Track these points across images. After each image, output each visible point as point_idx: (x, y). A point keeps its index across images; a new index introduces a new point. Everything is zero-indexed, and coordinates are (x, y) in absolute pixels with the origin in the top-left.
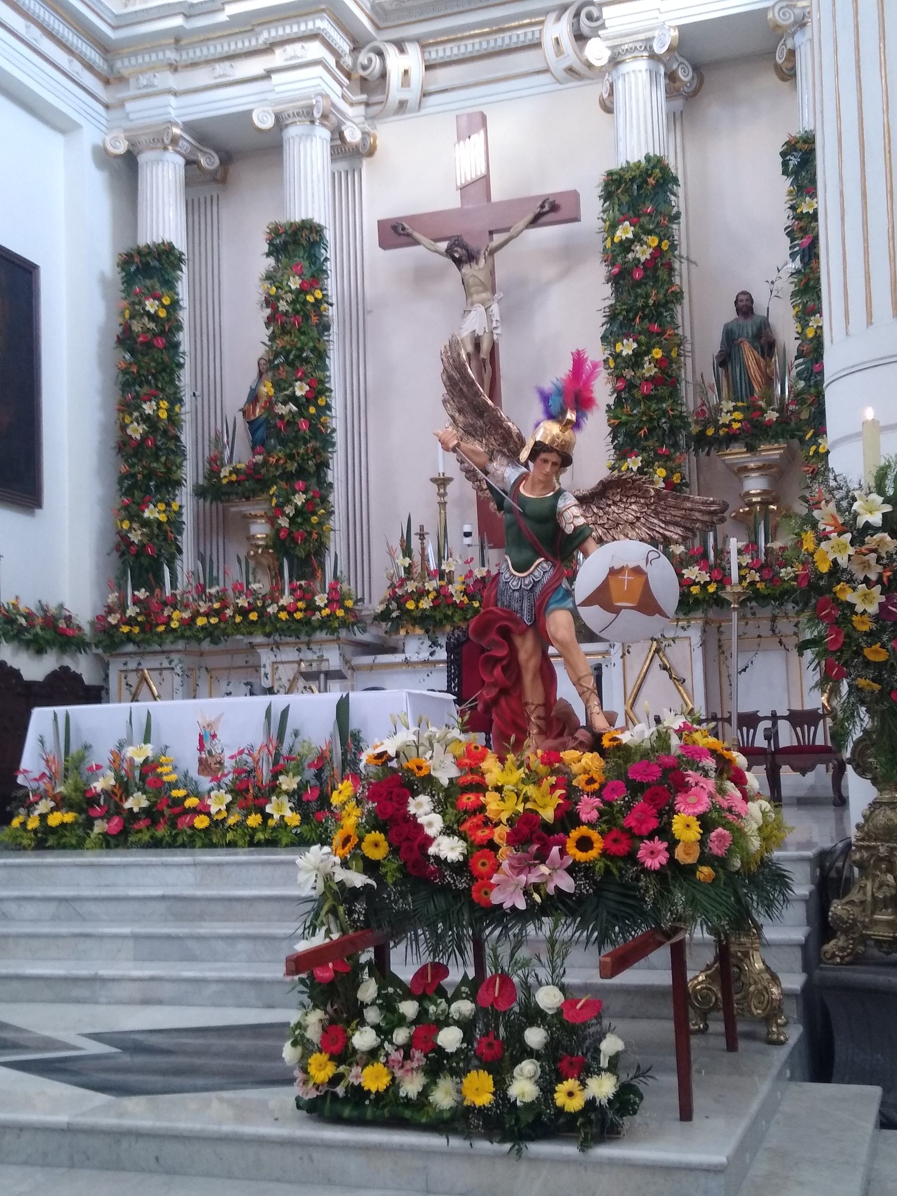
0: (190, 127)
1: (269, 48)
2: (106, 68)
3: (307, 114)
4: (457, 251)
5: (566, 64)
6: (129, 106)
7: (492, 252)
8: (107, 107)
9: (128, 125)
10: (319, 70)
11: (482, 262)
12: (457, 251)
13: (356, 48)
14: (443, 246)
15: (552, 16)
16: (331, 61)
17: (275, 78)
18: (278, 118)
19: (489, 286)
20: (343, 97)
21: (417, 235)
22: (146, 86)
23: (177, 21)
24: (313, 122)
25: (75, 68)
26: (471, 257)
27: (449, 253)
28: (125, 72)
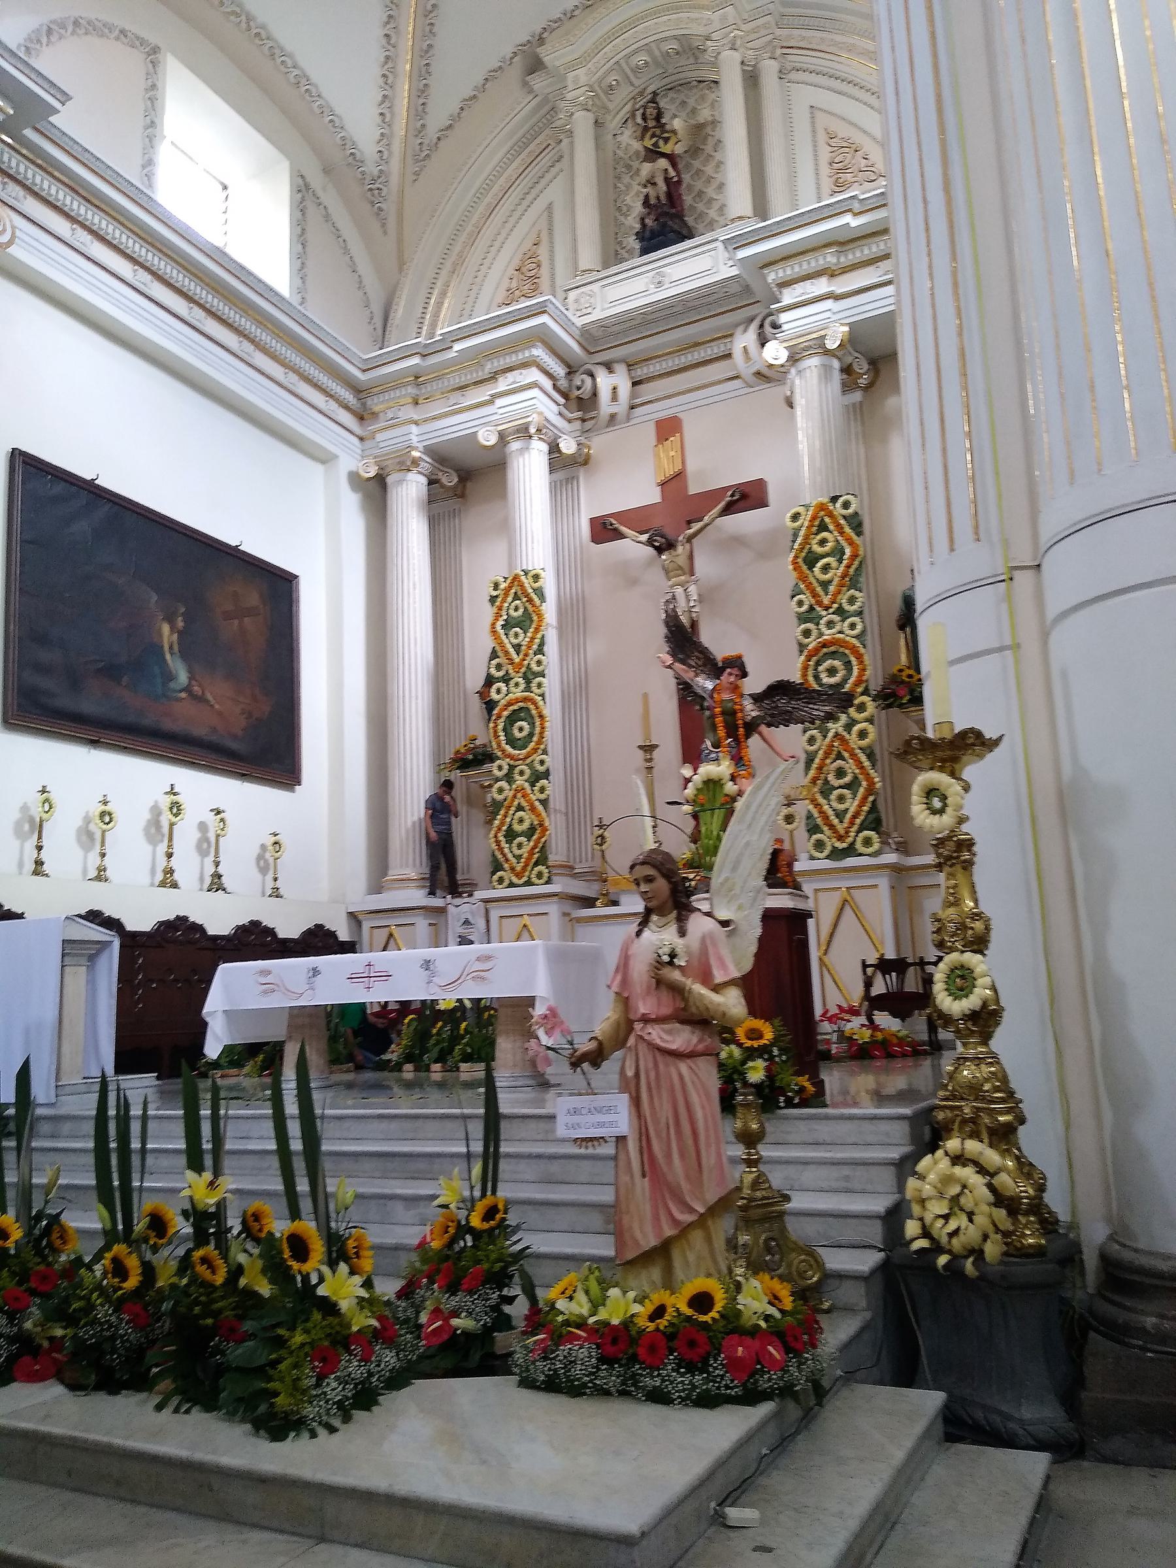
0: (428, 450)
1: (493, 377)
2: (359, 405)
3: (523, 432)
4: (655, 541)
5: (754, 369)
6: (380, 437)
7: (689, 539)
8: (361, 439)
9: (376, 451)
10: (535, 392)
11: (680, 549)
12: (655, 541)
13: (571, 372)
14: (644, 537)
15: (741, 328)
16: (547, 384)
17: (500, 402)
18: (502, 436)
19: (687, 569)
20: (560, 414)
21: (624, 529)
22: (392, 419)
23: (416, 360)
24: (530, 437)
25: (332, 407)
26: (670, 546)
27: (650, 542)
28: (376, 409)
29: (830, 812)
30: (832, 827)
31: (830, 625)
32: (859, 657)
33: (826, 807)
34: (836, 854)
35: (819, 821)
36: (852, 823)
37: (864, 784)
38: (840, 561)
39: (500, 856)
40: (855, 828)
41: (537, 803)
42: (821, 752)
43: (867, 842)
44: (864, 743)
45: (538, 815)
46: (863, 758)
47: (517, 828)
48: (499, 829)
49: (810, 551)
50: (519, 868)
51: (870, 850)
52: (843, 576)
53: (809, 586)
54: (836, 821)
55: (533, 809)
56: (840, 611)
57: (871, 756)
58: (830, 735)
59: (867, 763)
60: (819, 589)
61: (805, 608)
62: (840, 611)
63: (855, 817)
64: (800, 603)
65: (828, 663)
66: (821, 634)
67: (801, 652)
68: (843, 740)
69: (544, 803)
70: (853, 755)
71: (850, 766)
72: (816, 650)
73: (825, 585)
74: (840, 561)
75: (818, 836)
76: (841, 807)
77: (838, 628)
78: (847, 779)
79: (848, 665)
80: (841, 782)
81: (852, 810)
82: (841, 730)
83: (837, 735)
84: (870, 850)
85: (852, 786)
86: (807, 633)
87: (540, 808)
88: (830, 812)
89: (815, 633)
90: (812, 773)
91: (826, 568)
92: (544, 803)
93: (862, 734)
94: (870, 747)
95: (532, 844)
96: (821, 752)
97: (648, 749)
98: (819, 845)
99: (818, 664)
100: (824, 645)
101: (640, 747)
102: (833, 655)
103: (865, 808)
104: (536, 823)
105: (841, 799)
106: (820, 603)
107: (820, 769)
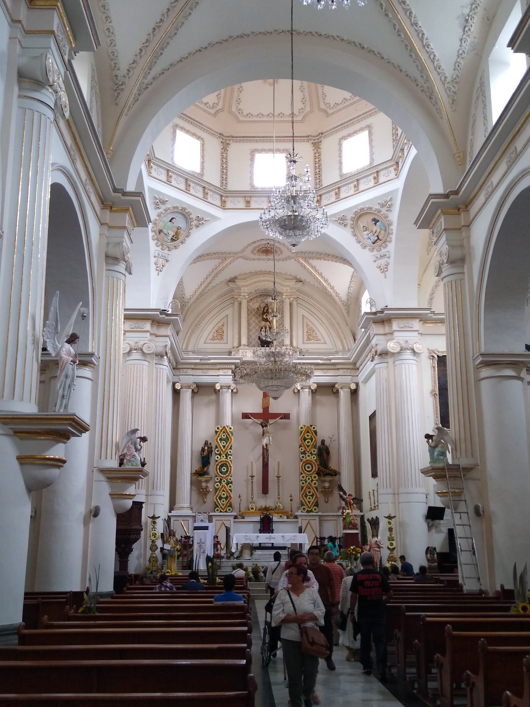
29: (307, 502)
30: (307, 505)
31: (309, 456)
32: (315, 465)
33: (306, 500)
34: (308, 512)
35: (304, 503)
36: (312, 504)
37: (315, 495)
38: (312, 441)
39: (217, 504)
40: (312, 506)
41: (228, 490)
42: (305, 487)
43: (315, 509)
44: (315, 486)
45: (229, 494)
46: (315, 489)
47: (223, 496)
48: (217, 496)
49: (305, 437)
50: (223, 507)
51: (316, 511)
52: (312, 445)
53: (304, 446)
54: (308, 504)
55: (227, 492)
56: (311, 453)
57: (317, 489)
58: (308, 483)
59: (316, 491)
60: (306, 447)
61: (303, 451)
62: (311, 453)
63: (313, 503)
64: (302, 449)
65: (308, 465)
66: (306, 458)
67: (301, 461)
68: (311, 485)
69: (231, 491)
70: (313, 488)
71: (312, 491)
72: (306, 461)
73: (308, 446)
74: (312, 441)
75: (304, 507)
76: (309, 500)
77: (310, 457)
78: (311, 494)
79: (312, 466)
80: (310, 494)
81: (312, 501)
82: (310, 482)
83: (309, 483)
84: (316, 511)
85: (312, 496)
86: (303, 457)
87: (229, 491)
88: (307, 502)
89: (305, 457)
90: (303, 491)
91: (308, 442)
92: (231, 491)
93: (315, 484)
94: (317, 487)
95: (227, 501)
96: (305, 487)
97: (252, 477)
98: (304, 509)
99: (305, 465)
100: (307, 461)
101: (250, 476)
102: (309, 463)
103: (315, 501)
104: (228, 495)
105: (309, 498)
106: (307, 451)
107: (305, 490)
